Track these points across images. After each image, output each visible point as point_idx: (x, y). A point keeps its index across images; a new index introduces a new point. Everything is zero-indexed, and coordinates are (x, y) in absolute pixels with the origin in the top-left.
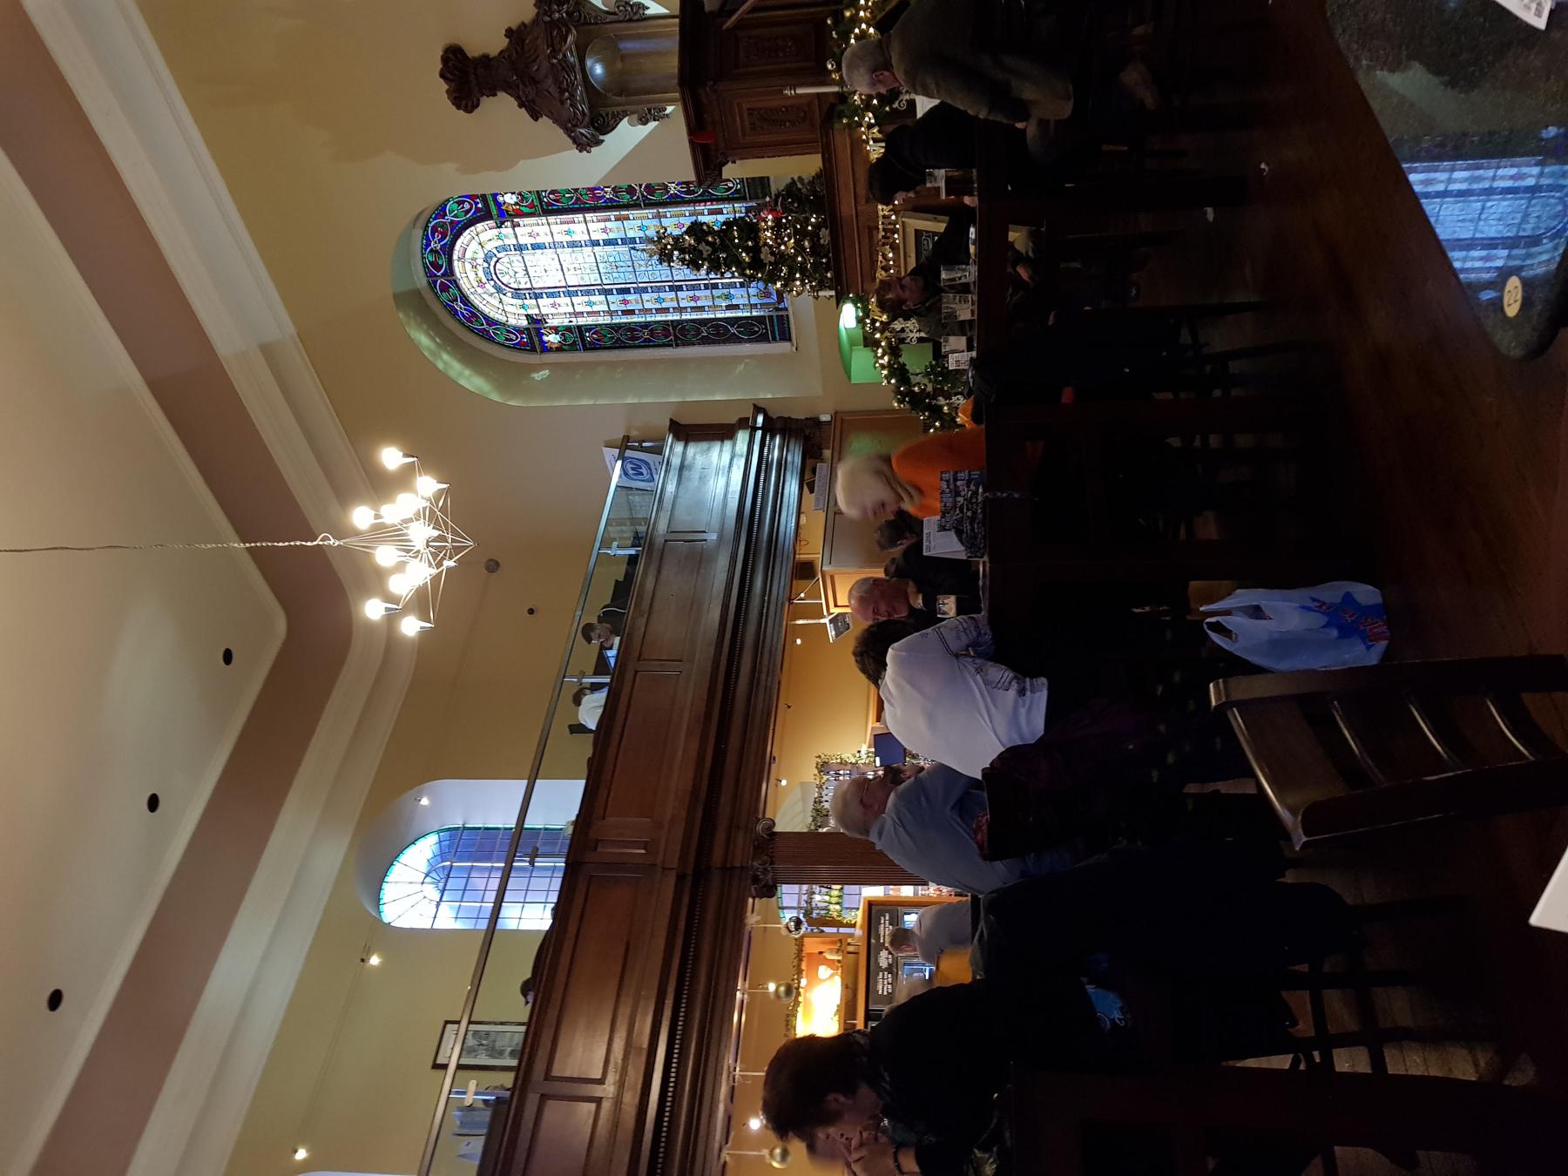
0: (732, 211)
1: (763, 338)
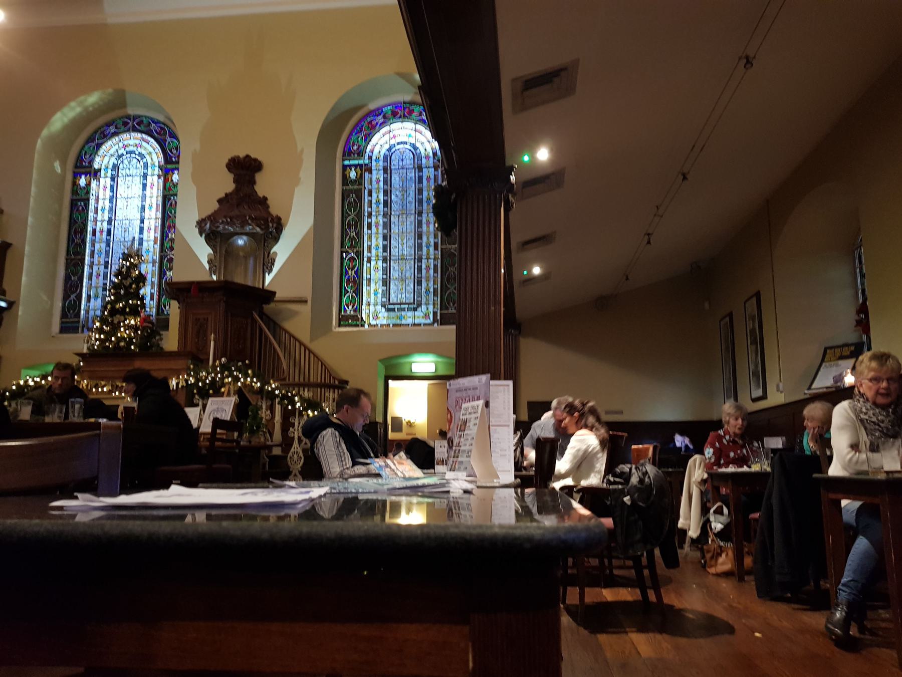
0: (151, 305)
1: (64, 315)
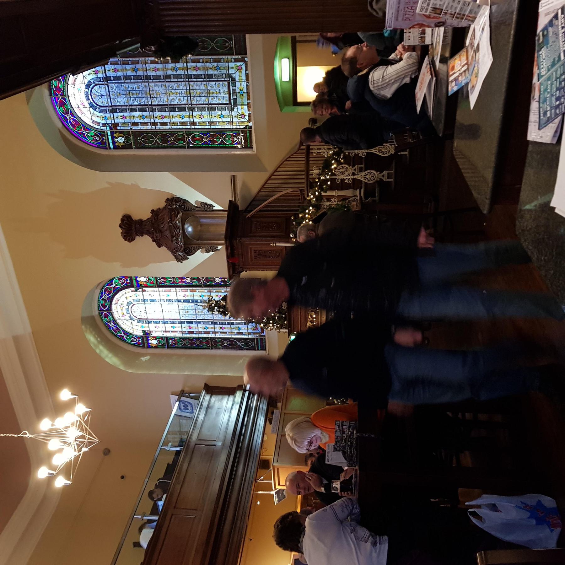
1: (253, 348)
